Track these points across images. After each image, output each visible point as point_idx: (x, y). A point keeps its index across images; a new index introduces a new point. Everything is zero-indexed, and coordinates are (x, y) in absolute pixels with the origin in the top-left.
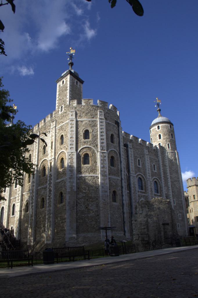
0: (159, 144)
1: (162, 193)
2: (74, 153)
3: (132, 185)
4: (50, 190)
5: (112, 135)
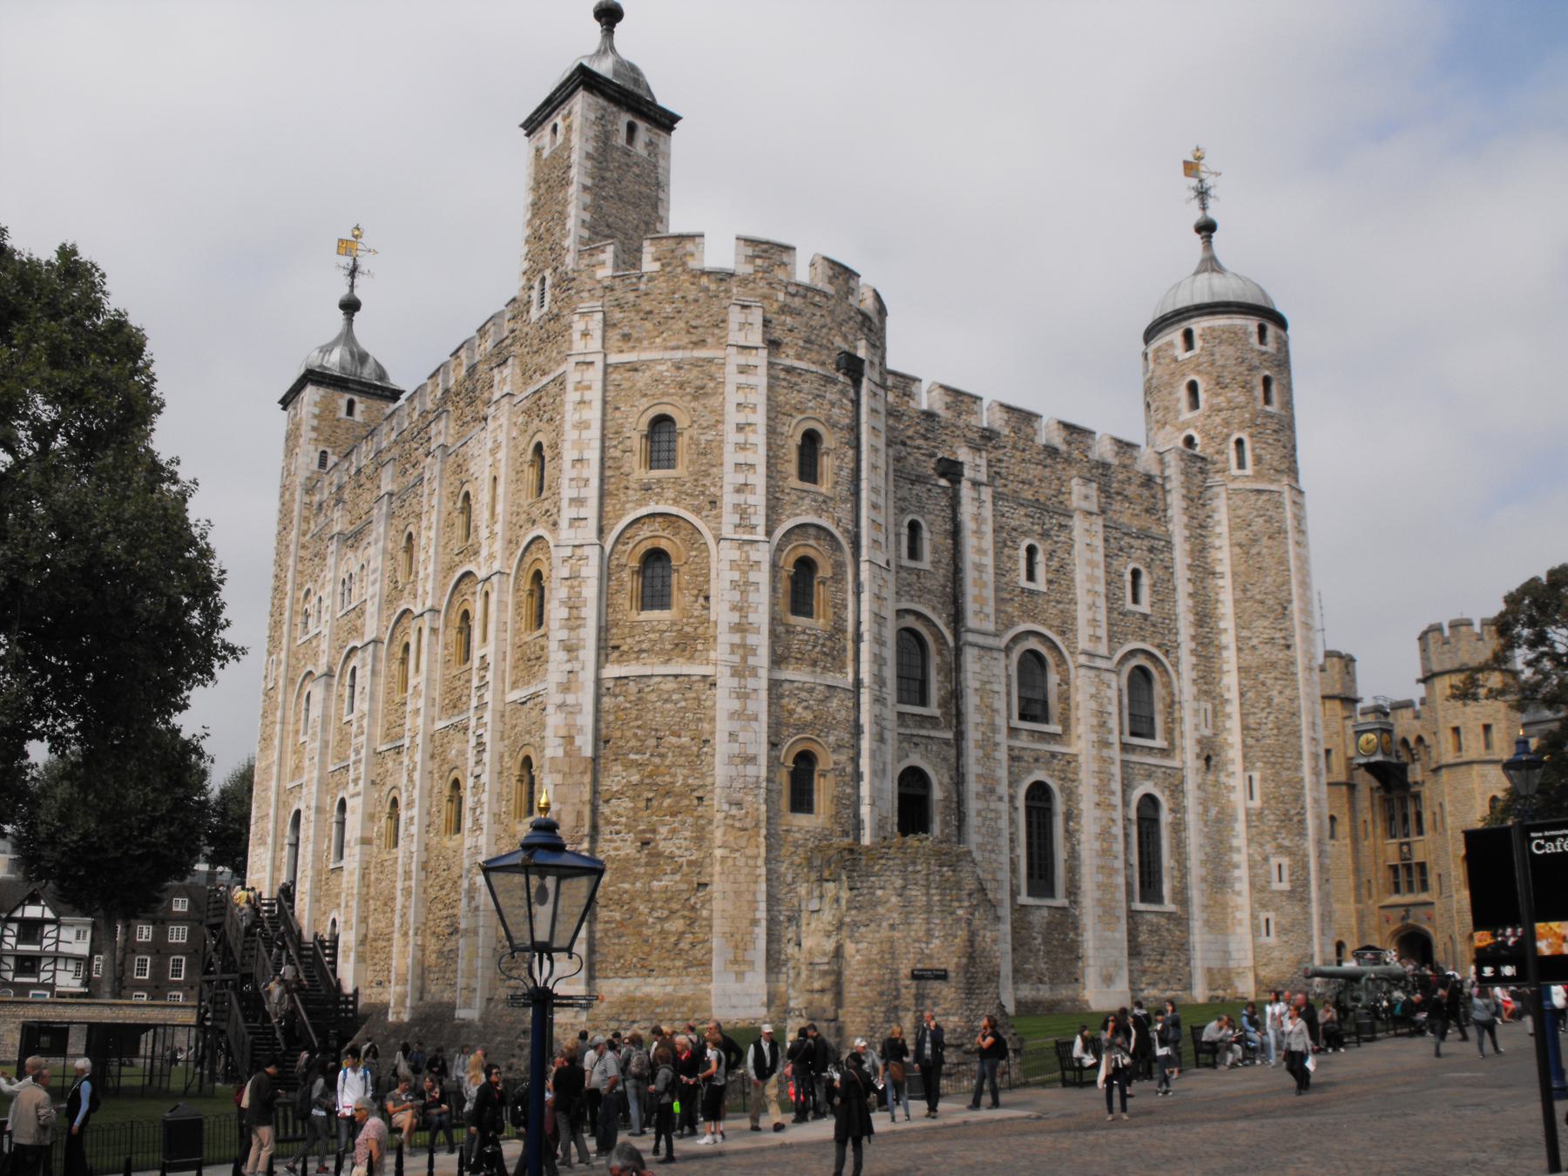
0: (1189, 441)
1: (1177, 733)
2: (587, 551)
3: (971, 701)
4: (479, 744)
5: (811, 440)
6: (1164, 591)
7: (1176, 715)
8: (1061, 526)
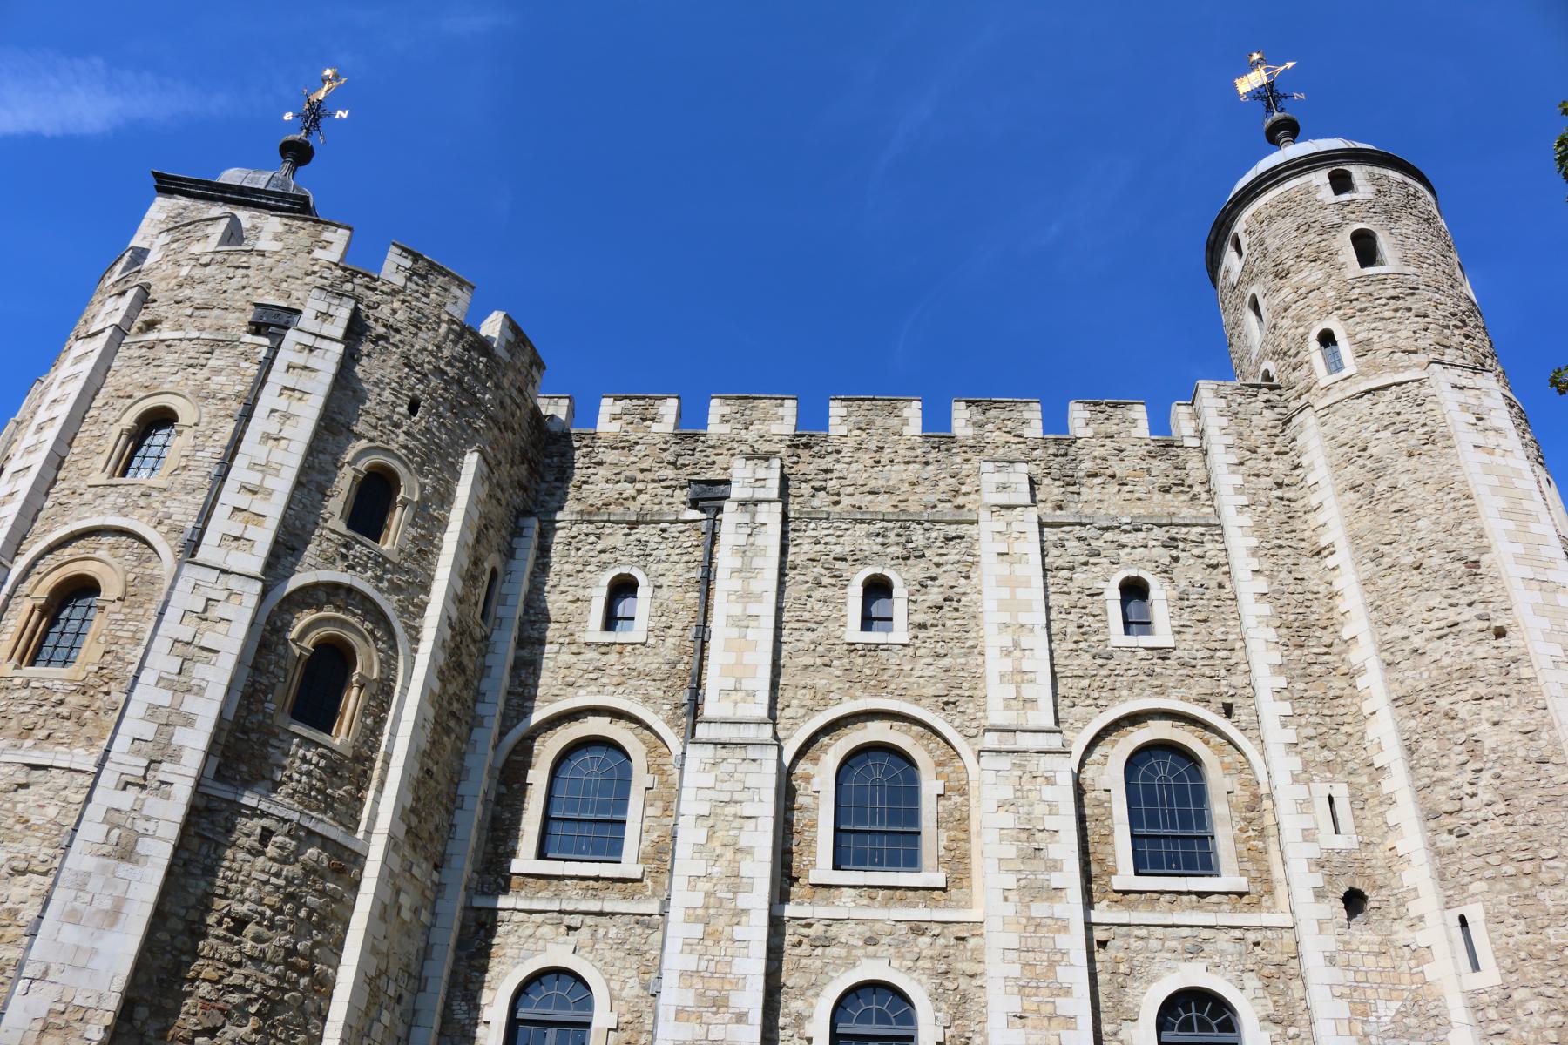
1: (1274, 857)
5: (160, 419)
6: (1211, 601)
7: (1269, 820)
8: (948, 539)
